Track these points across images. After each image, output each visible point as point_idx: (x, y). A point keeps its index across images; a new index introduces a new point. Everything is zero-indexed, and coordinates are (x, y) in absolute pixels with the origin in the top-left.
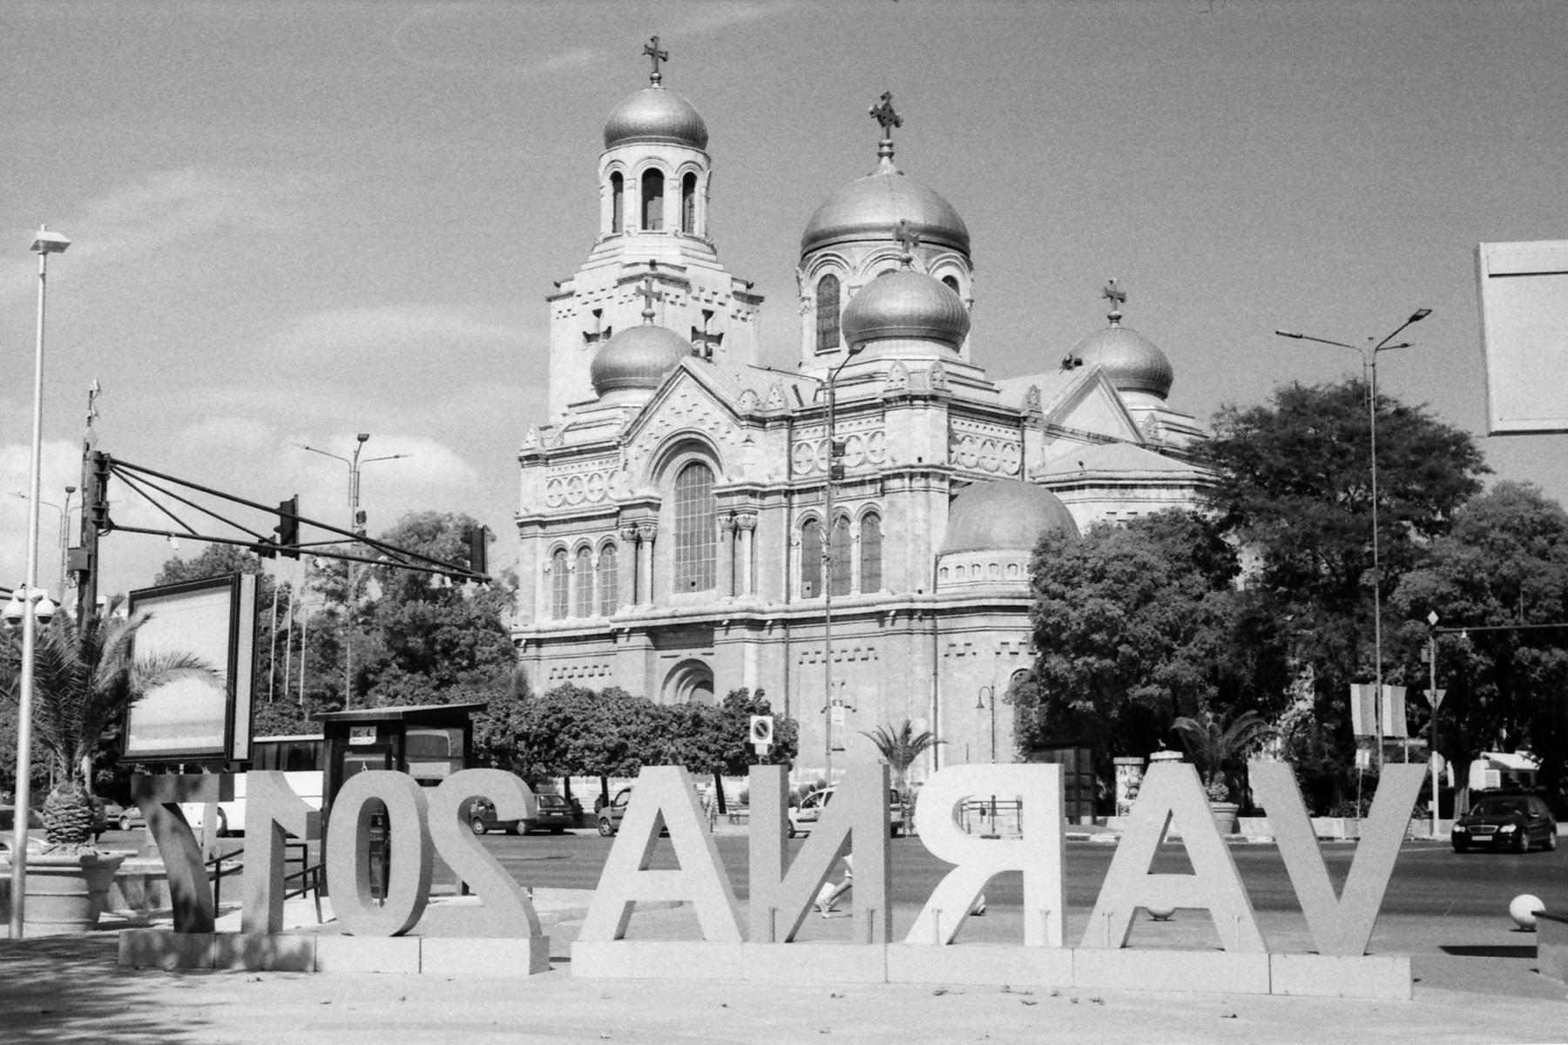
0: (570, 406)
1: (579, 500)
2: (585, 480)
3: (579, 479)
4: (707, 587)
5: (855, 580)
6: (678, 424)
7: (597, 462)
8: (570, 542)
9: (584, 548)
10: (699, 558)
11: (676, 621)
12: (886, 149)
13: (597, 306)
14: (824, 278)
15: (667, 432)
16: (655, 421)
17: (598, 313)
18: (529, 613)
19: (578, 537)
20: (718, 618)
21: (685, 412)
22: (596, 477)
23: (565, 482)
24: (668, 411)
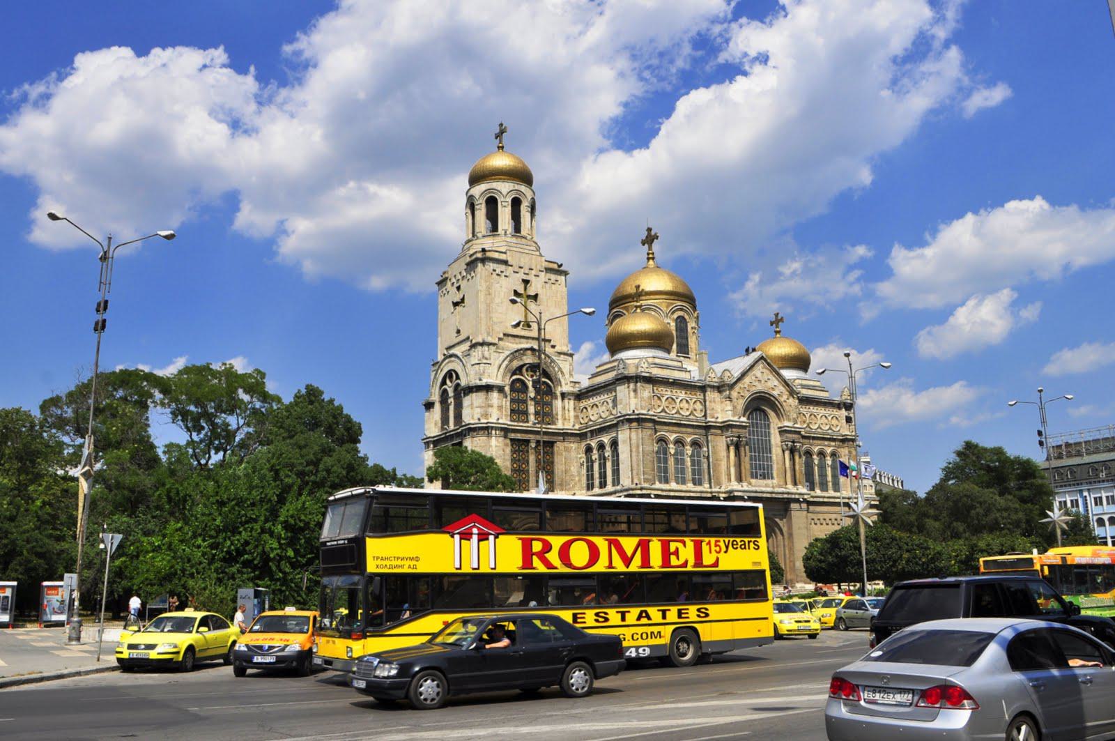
0: (504, 335)
1: (674, 411)
2: (678, 401)
3: (673, 399)
4: (769, 478)
5: (830, 484)
6: (759, 387)
7: (683, 392)
8: (672, 437)
9: (679, 442)
10: (763, 461)
11: (774, 496)
12: (651, 256)
13: (525, 277)
14: (679, 317)
15: (754, 390)
16: (747, 380)
17: (526, 282)
18: (650, 477)
19: (677, 435)
20: (797, 496)
21: (763, 382)
22: (684, 401)
23: (664, 399)
24: (753, 378)
